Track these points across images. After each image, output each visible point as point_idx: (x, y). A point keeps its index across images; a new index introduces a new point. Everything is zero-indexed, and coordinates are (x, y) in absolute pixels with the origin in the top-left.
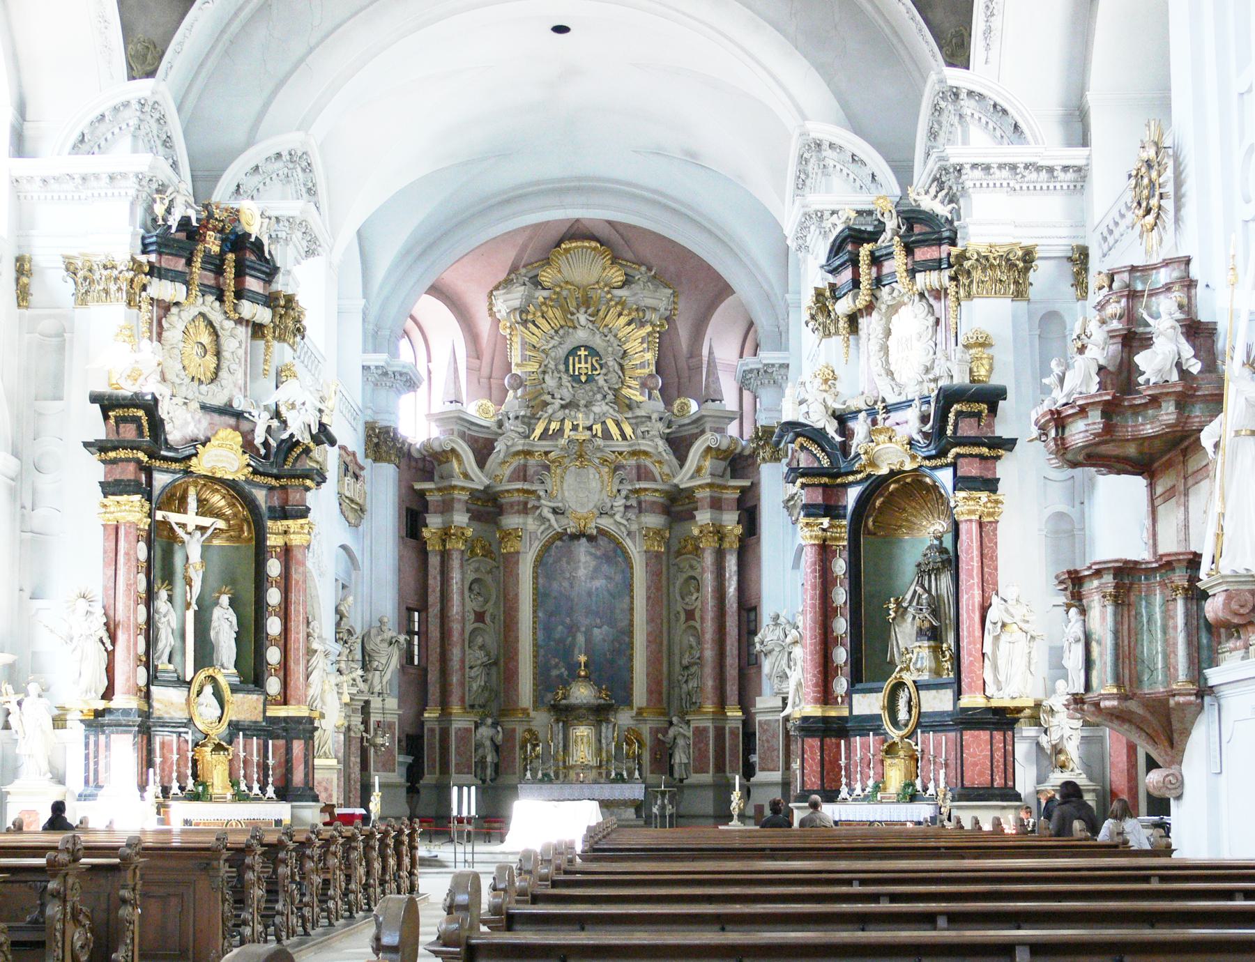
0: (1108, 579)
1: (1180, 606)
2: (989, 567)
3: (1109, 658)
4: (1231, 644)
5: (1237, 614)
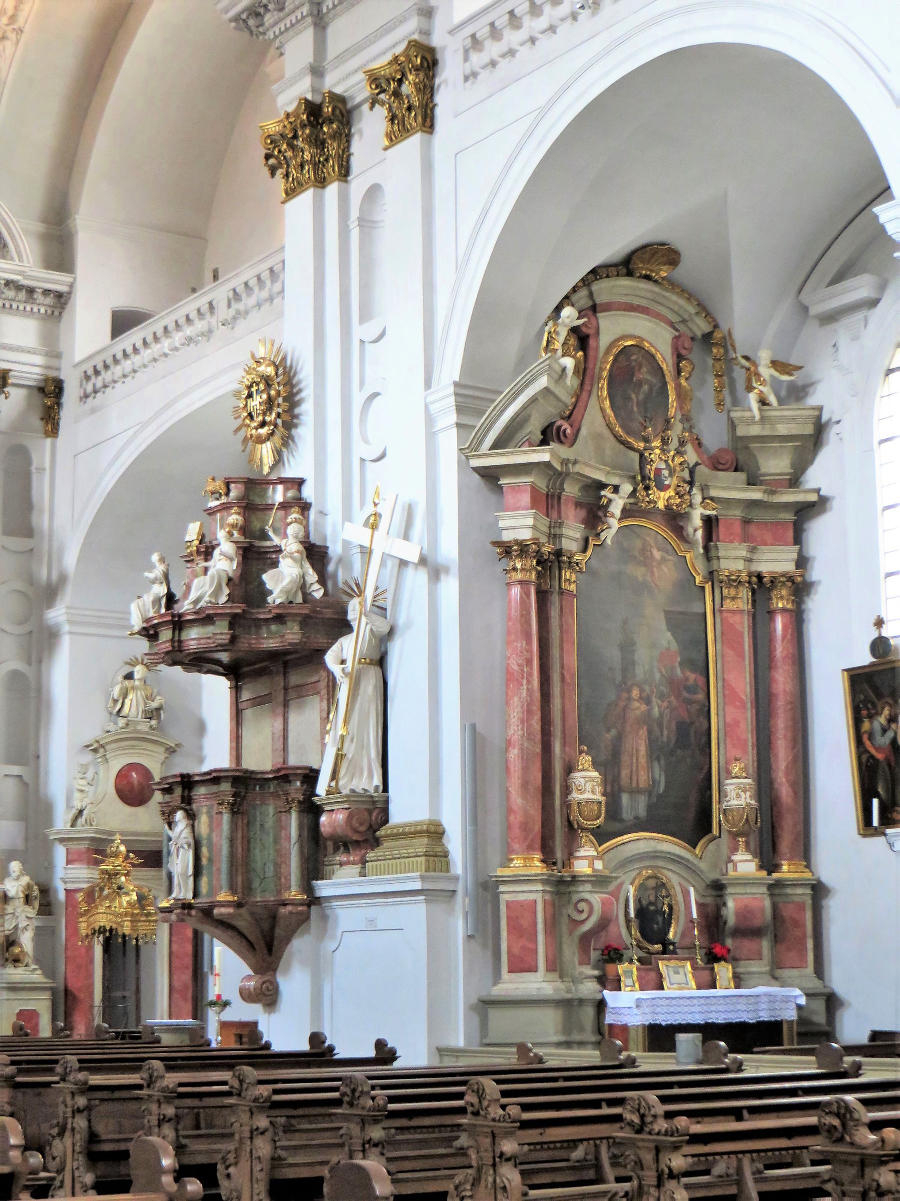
0: (226, 787)
1: (294, 819)
3: (224, 866)
4: (341, 857)
5: (356, 831)
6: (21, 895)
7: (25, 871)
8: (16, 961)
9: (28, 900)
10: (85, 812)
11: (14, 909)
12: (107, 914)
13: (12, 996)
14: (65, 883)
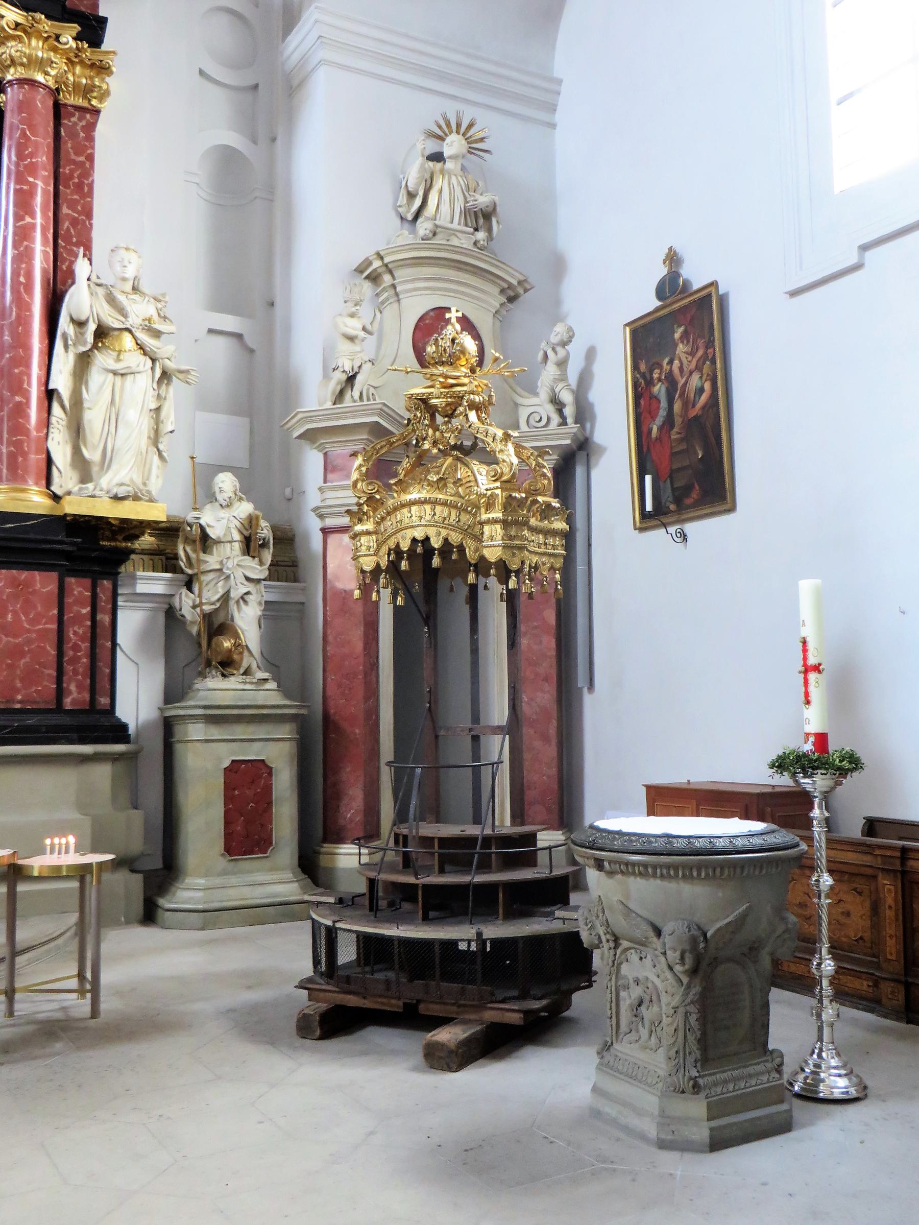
2: (72, 205)
6: (237, 536)
7: (246, 491)
8: (227, 665)
9: (250, 545)
10: (359, 379)
11: (221, 562)
12: (434, 503)
13: (215, 732)
14: (321, 517)
